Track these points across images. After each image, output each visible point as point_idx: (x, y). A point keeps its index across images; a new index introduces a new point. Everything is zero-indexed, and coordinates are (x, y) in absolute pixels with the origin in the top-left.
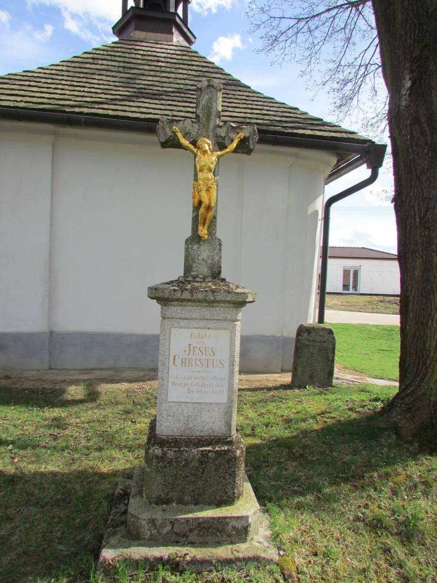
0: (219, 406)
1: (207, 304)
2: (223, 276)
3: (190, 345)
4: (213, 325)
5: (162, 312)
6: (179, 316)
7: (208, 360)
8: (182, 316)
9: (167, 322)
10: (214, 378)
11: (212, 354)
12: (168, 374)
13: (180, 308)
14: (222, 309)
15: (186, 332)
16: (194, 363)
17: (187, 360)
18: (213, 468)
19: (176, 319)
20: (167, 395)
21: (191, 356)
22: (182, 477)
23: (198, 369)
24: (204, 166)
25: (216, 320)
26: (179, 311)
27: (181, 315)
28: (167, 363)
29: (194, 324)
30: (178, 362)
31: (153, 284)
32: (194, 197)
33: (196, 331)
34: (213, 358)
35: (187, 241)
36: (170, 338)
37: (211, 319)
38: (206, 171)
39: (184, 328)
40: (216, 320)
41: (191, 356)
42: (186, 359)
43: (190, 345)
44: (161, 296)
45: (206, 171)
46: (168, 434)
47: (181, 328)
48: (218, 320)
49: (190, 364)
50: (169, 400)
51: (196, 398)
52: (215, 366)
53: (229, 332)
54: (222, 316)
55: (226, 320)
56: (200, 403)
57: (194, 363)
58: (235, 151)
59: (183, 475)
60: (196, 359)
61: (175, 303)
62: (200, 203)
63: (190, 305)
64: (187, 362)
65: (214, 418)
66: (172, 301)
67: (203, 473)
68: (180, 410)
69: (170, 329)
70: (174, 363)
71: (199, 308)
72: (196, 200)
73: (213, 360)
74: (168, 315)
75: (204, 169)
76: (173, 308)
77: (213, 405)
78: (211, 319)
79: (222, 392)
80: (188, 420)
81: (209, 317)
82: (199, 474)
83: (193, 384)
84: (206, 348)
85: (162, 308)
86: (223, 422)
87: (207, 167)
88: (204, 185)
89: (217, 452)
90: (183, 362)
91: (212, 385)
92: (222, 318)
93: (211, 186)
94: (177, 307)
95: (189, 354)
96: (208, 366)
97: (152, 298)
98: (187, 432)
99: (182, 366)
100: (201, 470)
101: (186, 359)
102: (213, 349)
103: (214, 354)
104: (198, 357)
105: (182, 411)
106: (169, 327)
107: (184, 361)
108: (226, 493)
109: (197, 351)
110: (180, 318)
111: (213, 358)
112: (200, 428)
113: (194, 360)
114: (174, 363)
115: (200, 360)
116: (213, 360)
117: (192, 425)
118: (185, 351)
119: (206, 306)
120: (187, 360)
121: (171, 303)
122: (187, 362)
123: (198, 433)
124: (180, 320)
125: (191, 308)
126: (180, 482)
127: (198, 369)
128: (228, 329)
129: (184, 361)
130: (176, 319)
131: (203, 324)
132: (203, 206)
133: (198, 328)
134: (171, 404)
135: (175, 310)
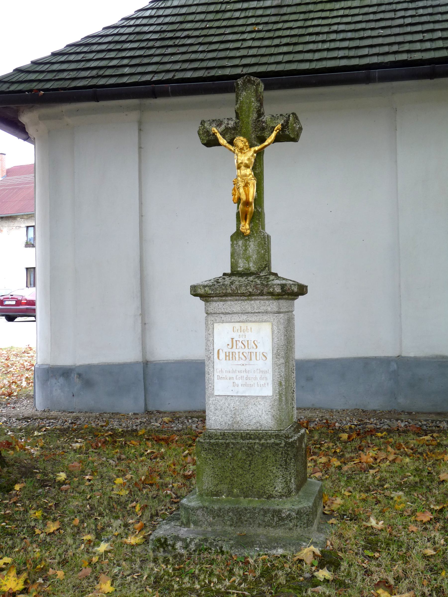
0: (265, 400)
1: (246, 298)
2: (273, 271)
3: (232, 339)
4: (254, 318)
5: (205, 309)
6: (220, 311)
7: (251, 353)
8: (223, 311)
9: (211, 318)
10: (258, 371)
11: (255, 347)
12: (213, 368)
13: (222, 303)
14: (262, 302)
15: (228, 327)
16: (237, 356)
17: (231, 354)
18: (260, 461)
19: (219, 314)
20: (213, 389)
21: (234, 350)
22: (230, 469)
23: (241, 362)
24: (241, 163)
25: (257, 313)
26: (220, 306)
27: (223, 310)
28: (212, 356)
29: (236, 317)
30: (222, 356)
31: (194, 283)
32: (234, 195)
33: (237, 325)
34: (256, 350)
35: (232, 237)
36: (213, 333)
37: (252, 313)
38: (243, 167)
39: (227, 322)
40: (257, 313)
41: (234, 350)
42: (229, 352)
43: (232, 339)
44: (206, 293)
45: (243, 167)
46: (216, 428)
47: (223, 323)
48: (259, 313)
49: (234, 358)
50: (215, 394)
51: (242, 391)
52: (258, 359)
53: (271, 323)
54: (262, 309)
55: (267, 312)
56: (246, 396)
57: (237, 356)
58: (277, 139)
59: (231, 467)
60: (239, 352)
61: (215, 298)
62: (239, 199)
63: (230, 300)
64: (231, 356)
65: (260, 412)
66: (213, 297)
67: (250, 466)
68: (227, 404)
69: (213, 324)
70: (218, 357)
71: (240, 302)
72: (236, 196)
73: (256, 353)
74: (210, 311)
75: (241, 167)
76: (214, 303)
77: (259, 398)
78: (252, 313)
79: (266, 385)
80: (235, 414)
81: (250, 311)
82: (247, 466)
83: (238, 377)
84: (248, 341)
85: (205, 305)
86: (270, 416)
87: (243, 164)
88: (242, 182)
89: (262, 445)
90: (227, 356)
91: (256, 378)
92: (263, 311)
93: (249, 181)
94: (218, 303)
95: (232, 348)
96: (251, 360)
97: (196, 295)
98: (235, 425)
99: (226, 360)
100: (248, 462)
101: (229, 352)
102: (255, 342)
103: (257, 347)
104: (241, 351)
105: (229, 405)
106: (212, 322)
107: (227, 354)
108: (275, 488)
109: (240, 344)
110: (223, 313)
111: (256, 350)
112: (247, 422)
113: (237, 354)
114: (218, 357)
115: (243, 353)
116: (256, 353)
117: (239, 419)
118: (228, 345)
119: (246, 300)
120: (231, 354)
121: (212, 298)
122: (231, 356)
123: (245, 427)
124: (222, 315)
125: (232, 303)
126: (228, 474)
127: (241, 362)
128: (269, 322)
129: (227, 354)
130: (219, 314)
131: (244, 317)
132: (242, 202)
133: (239, 322)
134: (218, 397)
135: (217, 305)
